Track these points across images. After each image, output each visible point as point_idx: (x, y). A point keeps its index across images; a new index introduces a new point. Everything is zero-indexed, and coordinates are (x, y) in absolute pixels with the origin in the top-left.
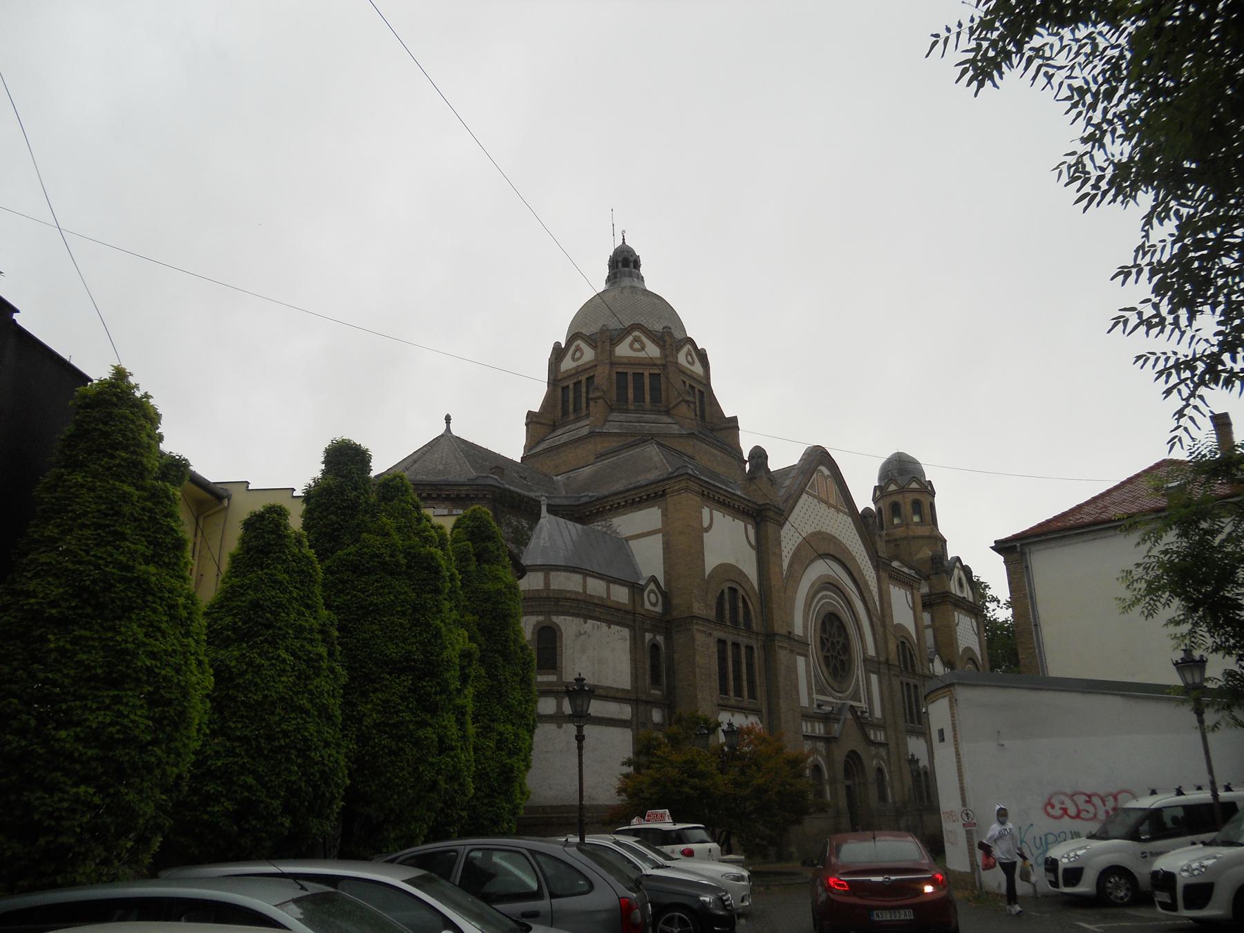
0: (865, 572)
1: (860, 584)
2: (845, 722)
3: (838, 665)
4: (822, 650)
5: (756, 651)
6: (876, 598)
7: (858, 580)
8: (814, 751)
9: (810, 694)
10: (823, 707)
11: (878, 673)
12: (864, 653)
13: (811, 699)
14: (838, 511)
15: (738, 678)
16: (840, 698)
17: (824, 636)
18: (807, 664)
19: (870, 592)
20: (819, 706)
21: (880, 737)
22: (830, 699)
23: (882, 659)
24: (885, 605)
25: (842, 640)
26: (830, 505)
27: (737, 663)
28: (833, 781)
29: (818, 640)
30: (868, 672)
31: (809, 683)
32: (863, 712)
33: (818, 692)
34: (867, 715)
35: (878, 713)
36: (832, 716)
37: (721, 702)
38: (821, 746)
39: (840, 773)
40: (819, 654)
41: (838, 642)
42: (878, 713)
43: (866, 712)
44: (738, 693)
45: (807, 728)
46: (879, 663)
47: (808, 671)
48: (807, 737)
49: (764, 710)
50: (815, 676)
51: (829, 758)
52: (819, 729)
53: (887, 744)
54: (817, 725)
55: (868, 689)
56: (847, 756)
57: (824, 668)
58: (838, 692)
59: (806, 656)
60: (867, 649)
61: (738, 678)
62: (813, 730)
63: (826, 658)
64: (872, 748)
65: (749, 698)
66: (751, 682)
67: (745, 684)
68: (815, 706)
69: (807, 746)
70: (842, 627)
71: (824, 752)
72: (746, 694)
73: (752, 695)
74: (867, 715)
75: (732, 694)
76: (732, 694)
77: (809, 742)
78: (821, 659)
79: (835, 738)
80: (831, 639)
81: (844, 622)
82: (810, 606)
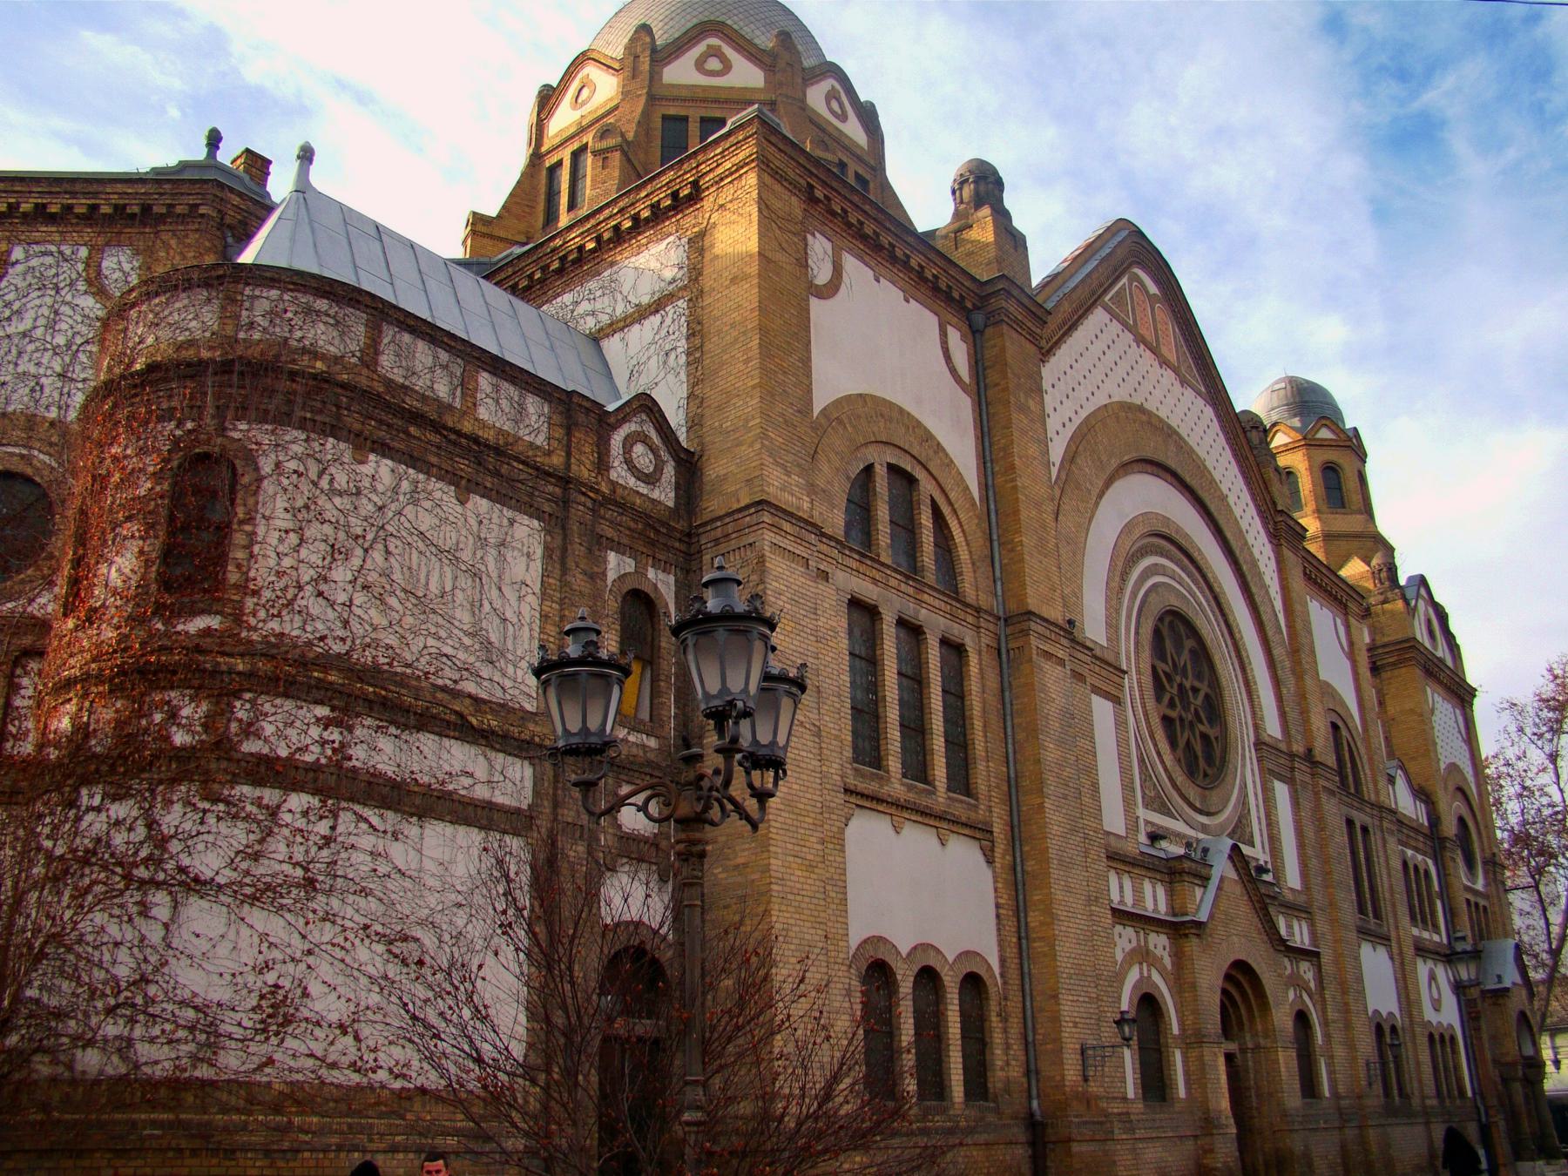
0: (1251, 541)
1: (1241, 560)
2: (1219, 888)
3: (1198, 747)
4: (1158, 699)
5: (973, 660)
6: (1278, 605)
7: (1237, 552)
8: (1142, 955)
9: (1129, 804)
10: (1164, 844)
11: (1290, 781)
12: (1256, 727)
13: (1132, 823)
14: (1184, 382)
15: (915, 728)
16: (1204, 829)
17: (1161, 666)
18: (1120, 724)
19: (1265, 588)
20: (1154, 837)
21: (1300, 935)
22: (1179, 826)
23: (1298, 748)
24: (1299, 625)
25: (1204, 688)
26: (1164, 363)
27: (914, 679)
28: (1193, 1040)
29: (1146, 667)
30: (1268, 774)
31: (1125, 771)
32: (1261, 870)
33: (1146, 806)
34: (1268, 877)
35: (1293, 879)
36: (1187, 865)
37: (852, 781)
38: (1159, 943)
39: (1213, 1022)
40: (1151, 704)
41: (1195, 690)
42: (1293, 879)
43: (1267, 871)
44: (918, 769)
45: (1121, 890)
46: (1292, 756)
47: (1122, 743)
48: (1121, 916)
49: (998, 828)
50: (1141, 761)
51: (1181, 979)
52: (1154, 899)
53: (1317, 955)
54: (1147, 886)
55: (1268, 815)
56: (1228, 977)
57: (1164, 746)
58: (1201, 812)
59: (1117, 701)
60: (1262, 719)
61: (915, 728)
62: (1138, 893)
63: (1167, 721)
64: (1286, 960)
65: (949, 789)
66: (959, 745)
67: (938, 743)
68: (1143, 838)
69: (1126, 938)
70: (1202, 654)
71: (1167, 961)
72: (940, 771)
73: (961, 780)
74: (1268, 877)
75: (894, 764)
76: (894, 764)
77: (1130, 931)
78: (1156, 721)
79: (1199, 924)
80: (1178, 679)
81: (1209, 643)
82: (1124, 580)
